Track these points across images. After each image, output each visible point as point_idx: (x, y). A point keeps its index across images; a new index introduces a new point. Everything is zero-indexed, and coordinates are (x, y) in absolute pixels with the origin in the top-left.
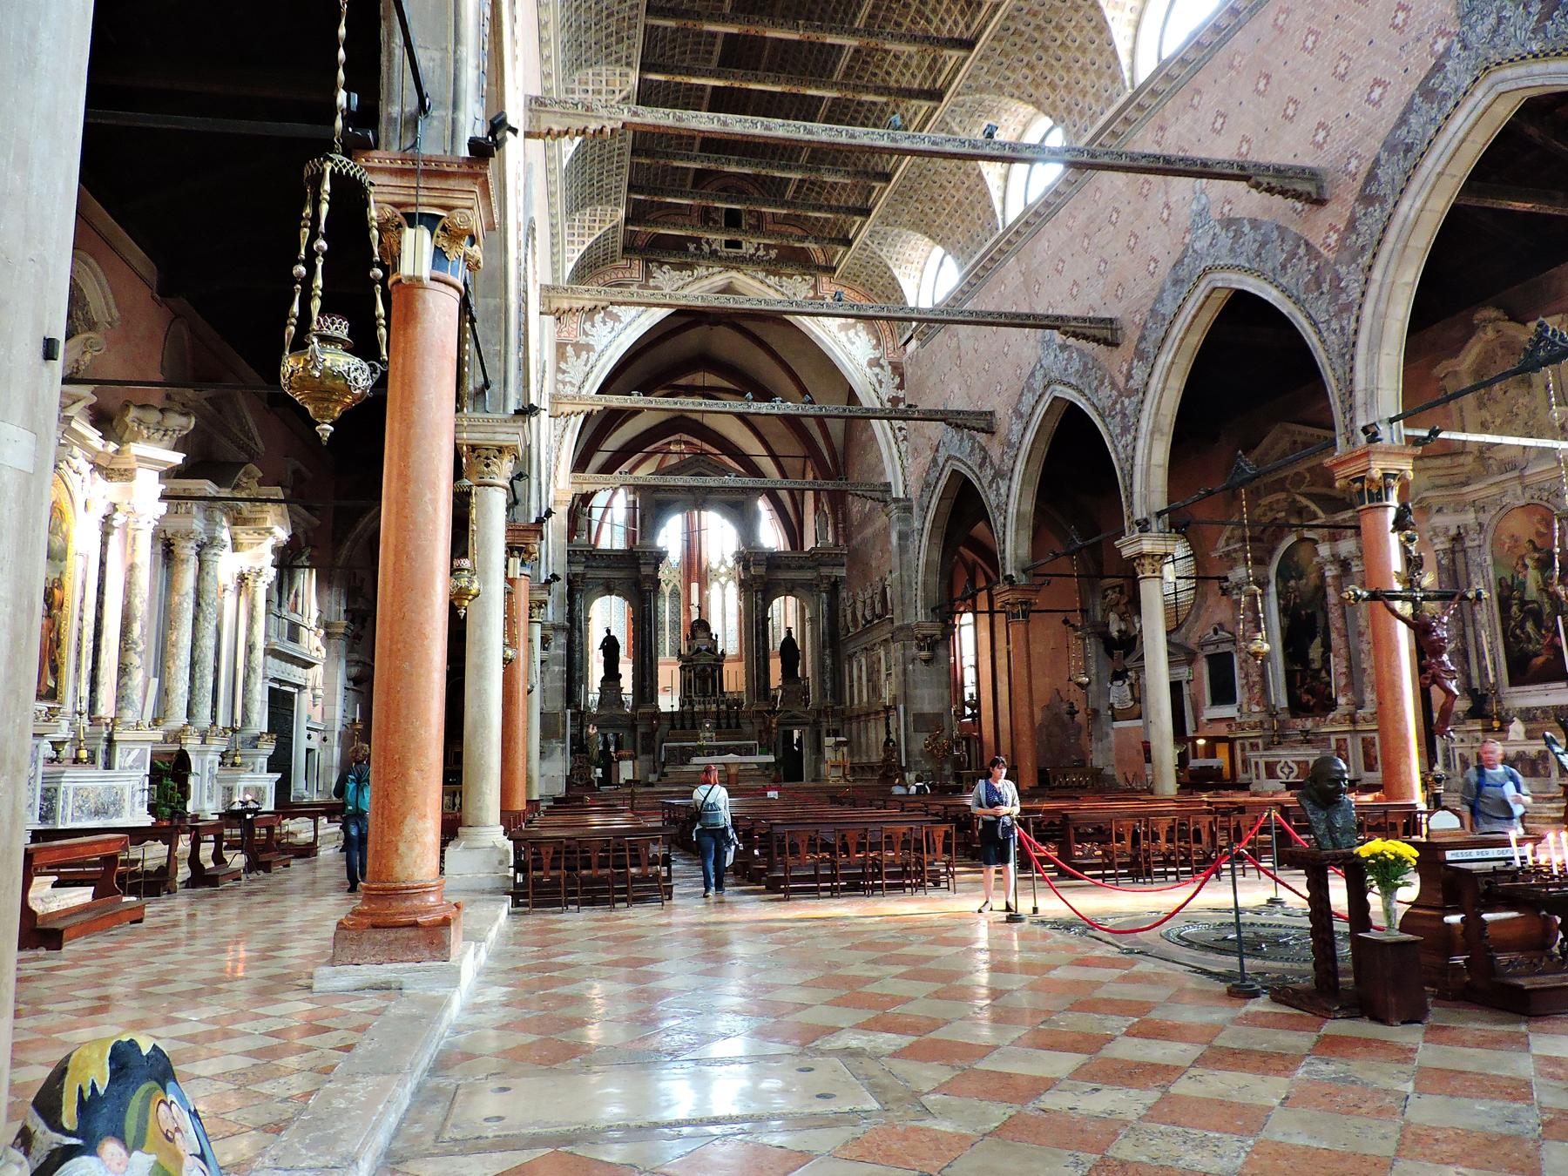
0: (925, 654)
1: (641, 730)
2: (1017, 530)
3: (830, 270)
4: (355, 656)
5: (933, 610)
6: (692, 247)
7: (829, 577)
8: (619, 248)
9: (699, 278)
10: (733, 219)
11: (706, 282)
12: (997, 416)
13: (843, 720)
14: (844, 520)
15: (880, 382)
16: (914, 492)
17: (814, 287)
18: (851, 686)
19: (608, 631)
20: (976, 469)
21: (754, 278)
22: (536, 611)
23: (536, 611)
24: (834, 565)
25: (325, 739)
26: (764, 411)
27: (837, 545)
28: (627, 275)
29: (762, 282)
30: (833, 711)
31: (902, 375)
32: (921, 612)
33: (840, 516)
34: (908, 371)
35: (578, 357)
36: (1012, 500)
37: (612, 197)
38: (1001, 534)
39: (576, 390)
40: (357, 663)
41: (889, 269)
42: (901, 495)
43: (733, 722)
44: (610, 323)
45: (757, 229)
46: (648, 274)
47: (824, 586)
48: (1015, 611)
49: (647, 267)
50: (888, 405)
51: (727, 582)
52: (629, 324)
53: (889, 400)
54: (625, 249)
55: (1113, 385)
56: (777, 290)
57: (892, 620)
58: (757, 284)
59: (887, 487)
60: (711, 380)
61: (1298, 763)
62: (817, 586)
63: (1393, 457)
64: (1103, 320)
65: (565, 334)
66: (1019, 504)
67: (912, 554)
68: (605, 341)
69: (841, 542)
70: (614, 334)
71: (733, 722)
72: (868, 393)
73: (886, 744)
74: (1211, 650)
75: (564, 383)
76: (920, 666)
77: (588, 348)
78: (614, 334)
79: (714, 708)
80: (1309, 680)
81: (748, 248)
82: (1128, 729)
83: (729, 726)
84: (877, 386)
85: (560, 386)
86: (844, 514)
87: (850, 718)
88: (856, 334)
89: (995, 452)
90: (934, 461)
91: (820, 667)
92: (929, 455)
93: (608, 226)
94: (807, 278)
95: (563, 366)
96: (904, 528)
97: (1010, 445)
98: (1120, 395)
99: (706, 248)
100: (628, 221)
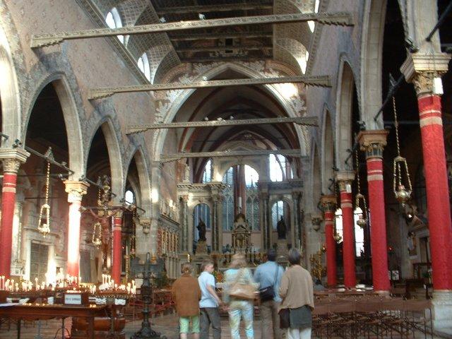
0: (316, 227)
3: (271, 57)
5: (318, 207)
6: (211, 55)
7: (296, 192)
10: (229, 42)
11: (217, 69)
15: (295, 104)
16: (309, 152)
17: (265, 66)
21: (237, 64)
31: (305, 100)
32: (313, 207)
34: (308, 99)
35: (163, 105)
42: (305, 154)
45: (240, 43)
46: (193, 68)
50: (299, 116)
53: (300, 112)
60: (245, 107)
63: (376, 136)
66: (325, 158)
68: (174, 98)
75: (158, 117)
76: (314, 232)
77: (168, 101)
81: (236, 52)
95: (157, 109)
99: (217, 54)
100: (176, 48)
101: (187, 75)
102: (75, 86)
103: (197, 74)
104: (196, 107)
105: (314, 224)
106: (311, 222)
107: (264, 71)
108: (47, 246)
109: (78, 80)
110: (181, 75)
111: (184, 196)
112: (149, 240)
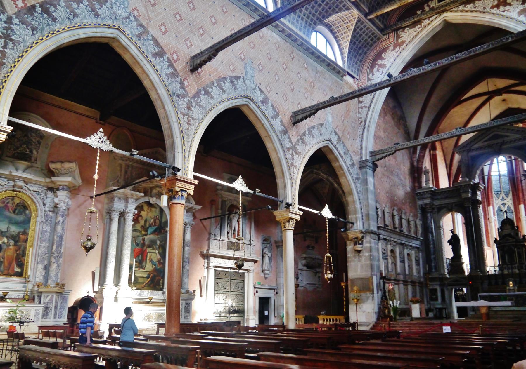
4: (304, 255)
8: (377, 32)
9: (425, 27)
11: (430, 27)
22: (287, 224)
23: (287, 224)
25: (277, 293)
28: (388, 42)
29: (462, 11)
37: (341, 6)
39: (367, 109)
40: (305, 258)
44: (381, 70)
46: (398, 37)
49: (397, 33)
54: (381, 30)
56: (472, 11)
58: (460, 14)
65: (361, 84)
70: (383, 74)
75: (362, 108)
78: (383, 74)
85: (360, 110)
93: (354, 22)
99: (427, 9)
101: (392, 48)
102: (153, 49)
103: (403, 42)
104: (426, 95)
108: (244, 274)
109: (162, 44)
110: (384, 50)
111: (426, 204)
112: (363, 259)
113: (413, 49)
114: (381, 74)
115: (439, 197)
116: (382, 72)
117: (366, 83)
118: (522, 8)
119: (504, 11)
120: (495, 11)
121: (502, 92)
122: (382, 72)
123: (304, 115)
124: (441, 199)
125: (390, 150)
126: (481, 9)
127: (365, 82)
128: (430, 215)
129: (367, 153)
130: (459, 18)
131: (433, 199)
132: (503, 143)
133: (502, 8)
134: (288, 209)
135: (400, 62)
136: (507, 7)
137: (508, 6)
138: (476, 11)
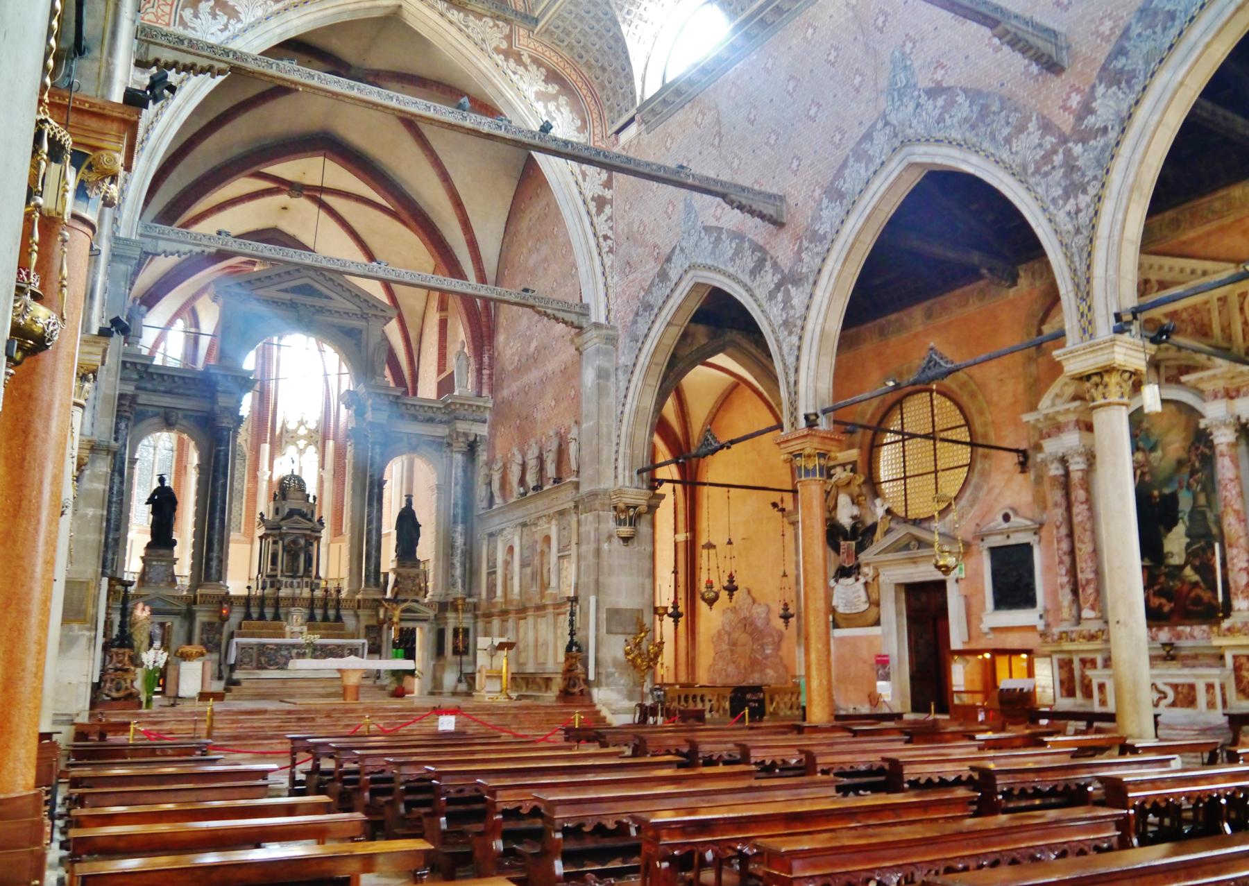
0: (625, 530)
1: (201, 617)
2: (819, 355)
3: (530, 20)
5: (639, 472)
7: (466, 435)
12: (792, 202)
13: (476, 617)
14: (491, 366)
17: (509, 38)
18: (492, 573)
19: (162, 480)
20: (746, 278)
24: (474, 420)
26: (485, 129)
27: (479, 395)
29: (442, 15)
30: (464, 604)
33: (486, 359)
36: (813, 313)
38: (791, 360)
41: (616, 23)
42: (603, 320)
43: (331, 613)
44: (223, 19)
47: (461, 445)
48: (810, 466)
51: (306, 446)
52: (252, 26)
53: (593, 199)
55: (1047, 127)
56: (461, 30)
57: (577, 486)
58: (436, 17)
59: (584, 310)
61: (1175, 687)
62: (450, 445)
64: (1047, 30)
67: (611, 400)
69: (485, 392)
71: (331, 613)
72: (568, 185)
73: (569, 649)
74: (998, 541)
76: (617, 544)
78: (227, 34)
79: (306, 593)
80: (1162, 579)
82: (860, 637)
83: (325, 618)
84: (580, 178)
86: (491, 358)
87: (488, 616)
88: (558, 108)
89: (783, 249)
90: (663, 276)
91: (447, 547)
92: (652, 268)
94: (501, 24)
96: (606, 365)
97: (816, 237)
98: (1064, 140)
105: (620, 522)
106: (612, 514)
107: (507, 54)
113: (315, 20)
114: (222, 31)
115: (149, 386)
116: (226, 27)
117: (168, 25)
118: (543, 89)
119: (515, 73)
120: (499, 59)
121: (305, 193)
122: (226, 27)
123: (189, 59)
124: (155, 391)
125: (205, 242)
126: (478, 39)
127: (166, 18)
128: (127, 426)
129: (133, 221)
130: (431, 24)
131: (137, 388)
132: (321, 310)
133: (512, 63)
134: (103, 340)
135: (278, 31)
136: (521, 70)
137: (522, 68)
138: (468, 37)
